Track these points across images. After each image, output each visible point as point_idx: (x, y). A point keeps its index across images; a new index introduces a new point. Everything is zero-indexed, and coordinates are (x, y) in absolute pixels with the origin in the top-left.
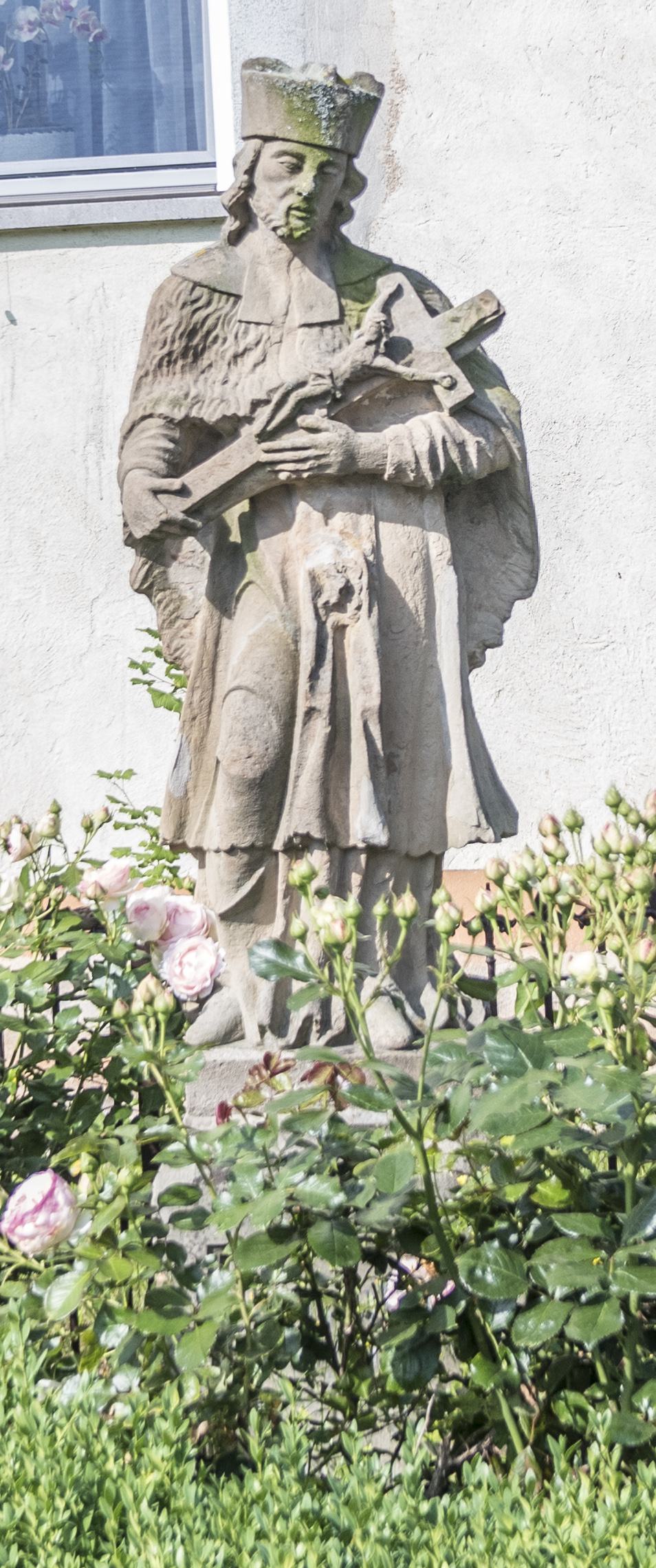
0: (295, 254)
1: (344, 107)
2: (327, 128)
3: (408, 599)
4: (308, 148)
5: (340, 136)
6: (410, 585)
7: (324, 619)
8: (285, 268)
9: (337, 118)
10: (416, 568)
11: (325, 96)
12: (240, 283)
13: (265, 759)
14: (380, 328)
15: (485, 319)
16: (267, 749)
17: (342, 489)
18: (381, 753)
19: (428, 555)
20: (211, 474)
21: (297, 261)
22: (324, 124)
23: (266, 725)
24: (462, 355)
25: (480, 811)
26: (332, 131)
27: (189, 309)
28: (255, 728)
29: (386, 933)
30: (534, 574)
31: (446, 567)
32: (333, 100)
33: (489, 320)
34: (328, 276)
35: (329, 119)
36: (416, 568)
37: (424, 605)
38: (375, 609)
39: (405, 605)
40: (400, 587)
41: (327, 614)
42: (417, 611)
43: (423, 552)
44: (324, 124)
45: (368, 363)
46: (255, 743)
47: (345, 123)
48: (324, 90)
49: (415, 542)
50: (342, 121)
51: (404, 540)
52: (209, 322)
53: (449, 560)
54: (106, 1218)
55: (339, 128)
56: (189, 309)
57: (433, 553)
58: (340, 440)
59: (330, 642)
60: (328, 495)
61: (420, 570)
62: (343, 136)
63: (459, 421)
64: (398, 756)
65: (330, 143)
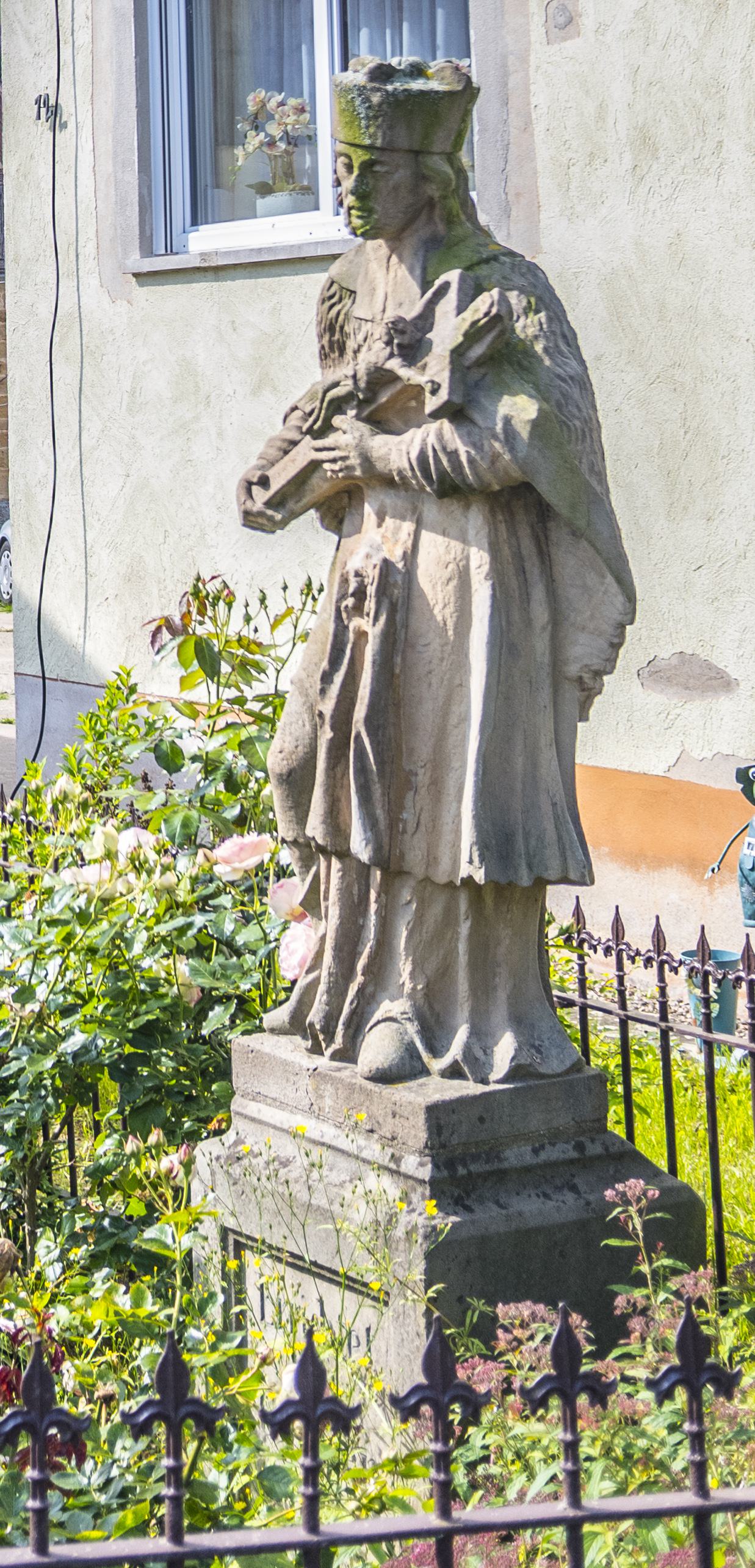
0: (393, 251)
1: (380, 105)
2: (367, 127)
3: (436, 611)
4: (353, 148)
5: (380, 134)
6: (440, 596)
7: (346, 622)
8: (385, 265)
9: (376, 117)
10: (449, 580)
11: (360, 95)
12: (355, 280)
13: (294, 757)
14: (389, 329)
15: (479, 320)
16: (296, 747)
17: (392, 492)
18: (374, 768)
19: (467, 568)
20: (284, 469)
21: (394, 259)
22: (363, 122)
23: (300, 722)
24: (474, 359)
25: (475, 848)
26: (372, 130)
27: (328, 304)
28: (291, 724)
29: (410, 959)
30: (630, 597)
31: (483, 581)
32: (367, 100)
33: (482, 322)
34: (418, 272)
35: (368, 118)
36: (449, 580)
37: (454, 619)
38: (383, 619)
39: (432, 616)
40: (429, 597)
41: (349, 619)
42: (445, 624)
43: (461, 564)
44: (363, 122)
45: (379, 365)
46: (288, 739)
47: (383, 121)
48: (359, 89)
49: (453, 552)
50: (380, 119)
51: (442, 550)
52: (341, 317)
53: (487, 575)
54: (221, 1177)
55: (378, 127)
56: (328, 304)
57: (473, 564)
58: (354, 442)
59: (349, 646)
60: (382, 497)
61: (454, 583)
62: (384, 134)
63: (457, 429)
64: (416, 775)
65: (367, 142)
